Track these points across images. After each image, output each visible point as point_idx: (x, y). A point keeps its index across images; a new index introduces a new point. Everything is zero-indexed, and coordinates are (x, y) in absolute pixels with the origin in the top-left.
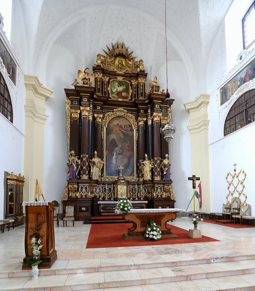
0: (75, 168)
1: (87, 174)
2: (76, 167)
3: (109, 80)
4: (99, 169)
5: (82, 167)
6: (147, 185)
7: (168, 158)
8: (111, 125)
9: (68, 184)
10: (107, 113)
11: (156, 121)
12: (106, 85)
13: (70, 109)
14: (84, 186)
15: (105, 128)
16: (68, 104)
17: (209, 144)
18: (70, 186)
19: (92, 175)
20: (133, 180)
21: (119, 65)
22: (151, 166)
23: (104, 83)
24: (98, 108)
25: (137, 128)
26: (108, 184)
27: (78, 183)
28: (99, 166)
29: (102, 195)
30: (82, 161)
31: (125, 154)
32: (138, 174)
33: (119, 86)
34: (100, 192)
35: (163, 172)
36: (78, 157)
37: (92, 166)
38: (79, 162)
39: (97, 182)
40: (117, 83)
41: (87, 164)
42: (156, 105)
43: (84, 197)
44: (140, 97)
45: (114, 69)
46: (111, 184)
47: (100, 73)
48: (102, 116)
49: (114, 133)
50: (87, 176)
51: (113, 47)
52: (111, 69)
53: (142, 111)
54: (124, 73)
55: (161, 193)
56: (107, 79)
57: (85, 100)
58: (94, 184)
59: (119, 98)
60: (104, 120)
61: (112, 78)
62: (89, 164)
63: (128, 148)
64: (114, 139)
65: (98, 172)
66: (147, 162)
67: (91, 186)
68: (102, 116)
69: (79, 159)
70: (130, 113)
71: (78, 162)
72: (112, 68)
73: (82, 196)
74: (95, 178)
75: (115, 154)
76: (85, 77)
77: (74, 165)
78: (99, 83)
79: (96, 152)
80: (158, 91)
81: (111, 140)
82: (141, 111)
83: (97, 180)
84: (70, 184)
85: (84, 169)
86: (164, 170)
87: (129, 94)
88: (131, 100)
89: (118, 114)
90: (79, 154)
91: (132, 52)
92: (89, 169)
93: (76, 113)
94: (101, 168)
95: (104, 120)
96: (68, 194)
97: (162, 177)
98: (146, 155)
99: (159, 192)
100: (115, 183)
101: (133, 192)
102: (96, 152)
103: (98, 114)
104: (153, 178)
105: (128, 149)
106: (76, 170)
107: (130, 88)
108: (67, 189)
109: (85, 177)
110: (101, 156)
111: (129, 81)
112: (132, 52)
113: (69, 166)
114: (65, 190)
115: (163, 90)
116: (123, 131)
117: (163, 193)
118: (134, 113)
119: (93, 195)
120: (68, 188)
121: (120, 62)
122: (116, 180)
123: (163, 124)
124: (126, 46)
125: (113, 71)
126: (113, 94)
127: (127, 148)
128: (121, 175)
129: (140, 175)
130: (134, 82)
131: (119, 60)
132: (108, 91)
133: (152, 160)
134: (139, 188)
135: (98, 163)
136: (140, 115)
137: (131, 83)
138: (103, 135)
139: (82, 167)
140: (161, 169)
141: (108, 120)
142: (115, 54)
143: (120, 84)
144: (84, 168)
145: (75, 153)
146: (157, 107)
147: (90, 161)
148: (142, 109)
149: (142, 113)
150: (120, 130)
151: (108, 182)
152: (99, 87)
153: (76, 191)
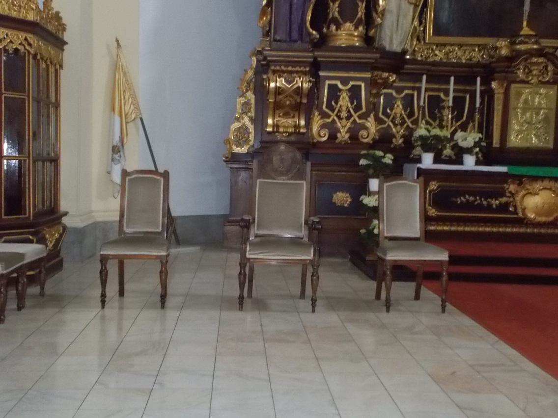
27: (315, 68)
43: (343, 135)
50: (361, 28)
73: (333, 137)
84: (274, 72)
96: (259, 121)
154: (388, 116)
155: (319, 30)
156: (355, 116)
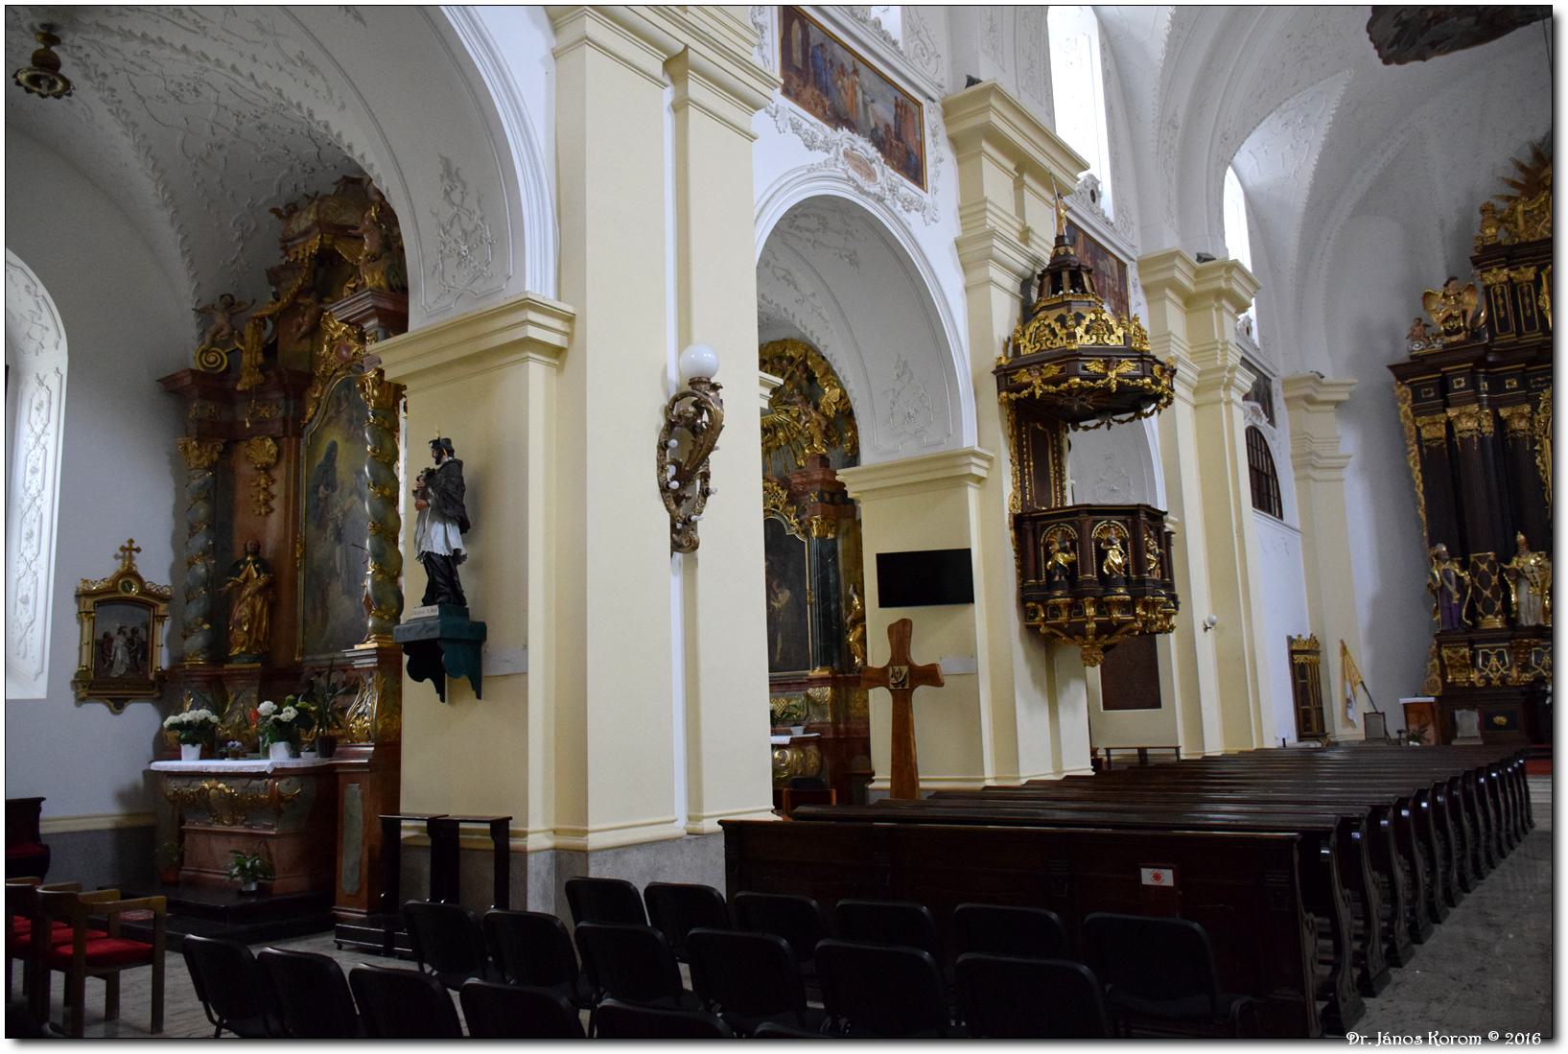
3: (1538, 276)
4: (1542, 590)
9: (1439, 646)
13: (1412, 417)
14: (1492, 649)
16: (1404, 401)
18: (1445, 652)
19: (1517, 612)
23: (1521, 289)
24: (1510, 384)
27: (1471, 644)
28: (1538, 579)
30: (1474, 571)
36: (1460, 559)
37: (1514, 582)
38: (1467, 578)
41: (1495, 579)
43: (1496, 683)
47: (1499, 268)
48: (1527, 409)
50: (1500, 617)
52: (1541, 233)
56: (1530, 274)
57: (1459, 383)
58: (1526, 641)
60: (1539, 414)
62: (1501, 580)
65: (1538, 599)
67: (1519, 645)
68: (1527, 409)
69: (1464, 567)
71: (1462, 577)
73: (1489, 680)
76: (1448, 313)
77: (1452, 588)
78: (1500, 302)
79: (1521, 537)
83: (1538, 626)
84: (1445, 648)
85: (1487, 597)
90: (1461, 551)
93: (1435, 423)
95: (1539, 414)
96: (1443, 676)
102: (1521, 537)
108: (1436, 661)
113: (1434, 592)
119: (1527, 677)
120: (1440, 658)
135: (1536, 569)
138: (1542, 468)
145: (1447, 550)
147: (1502, 570)
152: (1502, 314)
153: (1466, 666)
154: (1539, 665)
155: (1473, 620)
156: (1502, 670)
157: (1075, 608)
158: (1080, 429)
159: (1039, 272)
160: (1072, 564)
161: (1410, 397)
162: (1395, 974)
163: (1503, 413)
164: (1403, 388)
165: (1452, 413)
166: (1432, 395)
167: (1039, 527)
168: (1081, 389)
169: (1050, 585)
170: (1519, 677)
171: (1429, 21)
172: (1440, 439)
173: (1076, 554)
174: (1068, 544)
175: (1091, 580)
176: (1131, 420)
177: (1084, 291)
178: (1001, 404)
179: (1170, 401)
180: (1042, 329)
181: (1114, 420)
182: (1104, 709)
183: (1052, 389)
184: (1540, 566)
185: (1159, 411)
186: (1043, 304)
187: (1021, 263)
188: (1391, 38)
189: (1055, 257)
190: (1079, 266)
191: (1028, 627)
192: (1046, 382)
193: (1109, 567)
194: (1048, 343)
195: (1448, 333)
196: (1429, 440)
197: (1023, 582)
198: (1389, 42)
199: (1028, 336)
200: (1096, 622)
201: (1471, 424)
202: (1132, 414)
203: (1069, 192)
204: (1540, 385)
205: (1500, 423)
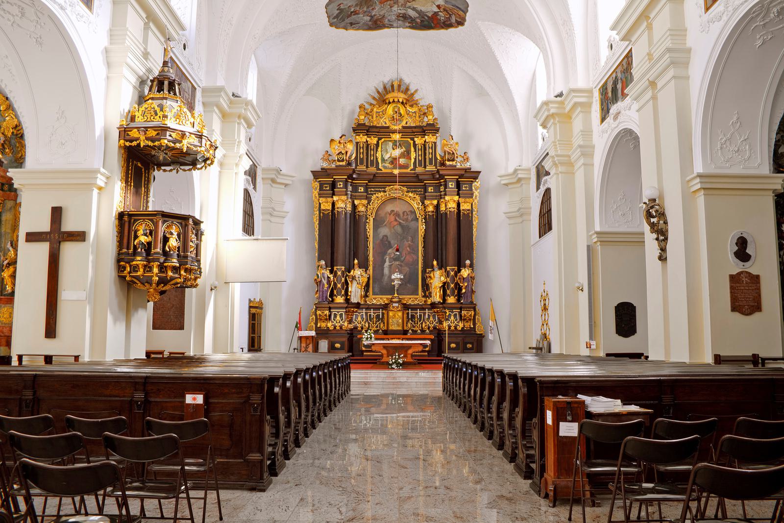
0: (326, 286)
1: (343, 295)
2: (328, 284)
3: (378, 142)
4: (362, 286)
5: (335, 284)
6: (435, 310)
7: (471, 266)
8: (382, 213)
9: (316, 310)
10: (375, 194)
11: (450, 208)
12: (374, 150)
14: (338, 312)
15: (372, 219)
16: (316, 189)
17: (532, 243)
18: (318, 312)
20: (416, 302)
21: (394, 115)
22: (443, 278)
25: (424, 216)
26: (374, 309)
27: (330, 308)
28: (361, 282)
29: (365, 326)
30: (335, 276)
31: (405, 258)
32: (424, 291)
33: (394, 149)
34: (363, 321)
35: (460, 289)
39: (358, 306)
40: (391, 144)
41: (343, 279)
42: (450, 183)
43: (338, 328)
44: (428, 166)
45: (386, 124)
46: (379, 309)
48: (365, 202)
49: (386, 225)
50: (343, 297)
51: (385, 88)
53: (431, 189)
54: (403, 127)
55: (456, 322)
57: (340, 185)
58: (352, 309)
59: (395, 168)
61: (382, 138)
62: (346, 280)
63: (410, 249)
64: (386, 236)
66: (437, 273)
67: (349, 312)
69: (331, 272)
70: (412, 192)
72: (384, 121)
73: (335, 327)
74: (354, 300)
75: (387, 259)
76: (339, 151)
77: (325, 282)
78: (362, 151)
79: (356, 261)
80: (453, 160)
81: (381, 237)
82: (430, 189)
84: (319, 310)
86: (462, 286)
87: (411, 159)
88: (414, 169)
89: (392, 195)
91: (416, 91)
92: (345, 286)
94: (364, 284)
96: (316, 324)
97: (459, 296)
98: (435, 263)
99: (452, 322)
100: (385, 307)
101: (415, 322)
103: (360, 199)
104: (444, 300)
105: (409, 250)
106: (327, 289)
107: (412, 149)
108: (314, 317)
109: (340, 299)
110: (364, 266)
111: (410, 138)
112: (416, 91)
113: (317, 283)
114: (311, 318)
115: (465, 153)
116: (400, 221)
117: (458, 322)
118: (419, 192)
119: (351, 326)
120: (316, 315)
121: (396, 110)
122: (386, 302)
123: (463, 210)
124: (405, 82)
125: (385, 125)
126: (385, 163)
127: (408, 248)
128: (396, 295)
129: (427, 293)
130: (419, 141)
131: (395, 107)
132: (377, 159)
133: (444, 270)
134: (425, 314)
135: (360, 277)
136: (428, 196)
137: (414, 142)
138: (368, 230)
139: (335, 284)
140: (457, 284)
141: (376, 206)
142: (387, 101)
143: (395, 144)
144: (339, 286)
146: (450, 186)
147: (347, 275)
148: (430, 186)
149: (431, 192)
150: (396, 220)
151: (376, 305)
152: (362, 156)
153: (326, 319)
157: (148, 268)
158: (161, 171)
159: (151, 78)
160: (149, 244)
161: (318, 188)
162: (298, 450)
163: (356, 202)
164: (316, 183)
165: (335, 198)
166: (328, 188)
167: (132, 221)
168: (167, 147)
169: (135, 253)
170: (348, 326)
171: (352, 12)
172: (329, 210)
173: (152, 238)
174: (148, 231)
175: (158, 253)
176: (190, 170)
177: (175, 94)
178: (120, 147)
179: (212, 163)
180: (149, 109)
181: (181, 169)
182: (153, 329)
183: (150, 143)
184: (362, 275)
185: (206, 167)
186: (152, 96)
187: (142, 71)
188: (335, 15)
189: (163, 71)
190: (174, 80)
191: (119, 276)
192: (147, 139)
193: (169, 247)
194: (152, 117)
195: (339, 161)
196: (324, 210)
197: (120, 250)
198: (333, 16)
199: (140, 112)
200: (159, 277)
201: (343, 205)
202: (191, 167)
203: (174, 40)
204: (372, 192)
205: (354, 207)
